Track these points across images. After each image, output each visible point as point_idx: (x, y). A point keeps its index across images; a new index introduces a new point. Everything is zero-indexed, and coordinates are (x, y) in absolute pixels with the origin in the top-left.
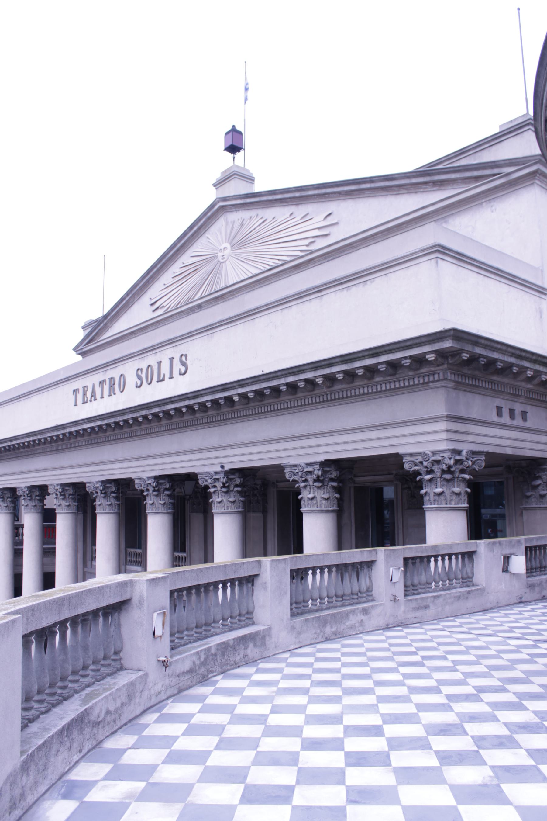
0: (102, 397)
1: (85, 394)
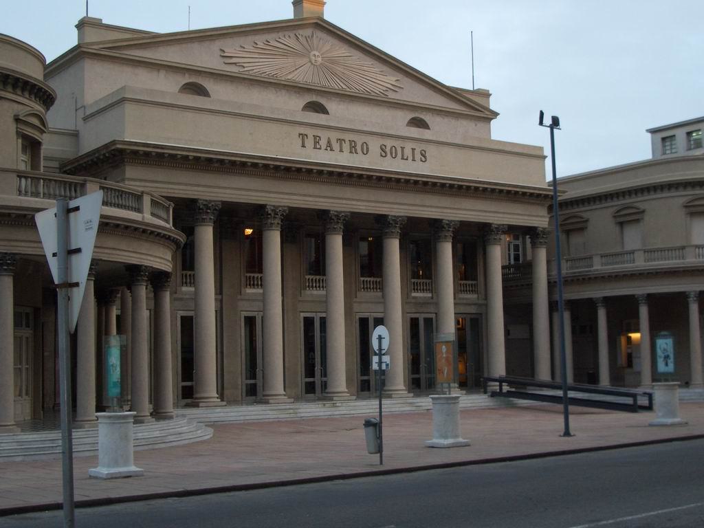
0: (341, 151)
1: (316, 143)
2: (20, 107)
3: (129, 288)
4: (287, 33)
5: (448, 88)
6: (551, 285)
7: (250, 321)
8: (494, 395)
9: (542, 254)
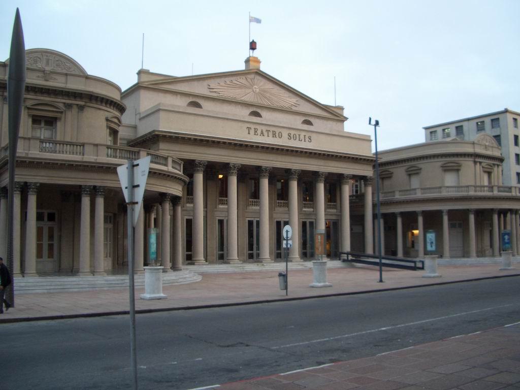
0: (268, 136)
1: (256, 132)
2: (109, 113)
3: (161, 204)
4: (242, 77)
5: (323, 105)
6: (374, 206)
7: (221, 222)
8: (344, 261)
9: (370, 190)
